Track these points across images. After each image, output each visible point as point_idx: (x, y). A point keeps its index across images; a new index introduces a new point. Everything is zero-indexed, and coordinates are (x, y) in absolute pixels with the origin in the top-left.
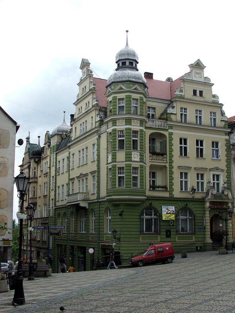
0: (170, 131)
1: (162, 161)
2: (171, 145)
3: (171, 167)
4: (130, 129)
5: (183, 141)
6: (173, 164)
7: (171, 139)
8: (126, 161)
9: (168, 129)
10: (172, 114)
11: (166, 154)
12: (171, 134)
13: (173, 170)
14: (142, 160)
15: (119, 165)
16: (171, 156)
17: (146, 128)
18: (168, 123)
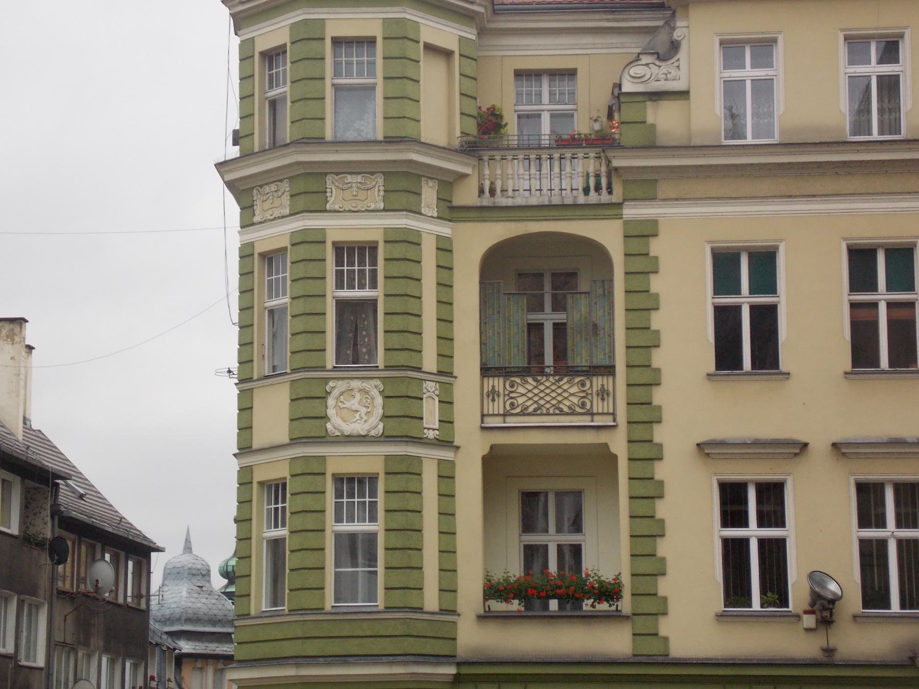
0: (631, 212)
1: (585, 421)
2: (644, 303)
3: (647, 453)
4: (315, 239)
5: (746, 269)
6: (660, 434)
7: (643, 267)
8: (295, 441)
9: (616, 197)
10: (657, 96)
11: (610, 370)
12: (641, 234)
13: (661, 471)
14: (401, 424)
15: (344, 460)
16: (645, 380)
17: (452, 212)
18: (616, 163)
